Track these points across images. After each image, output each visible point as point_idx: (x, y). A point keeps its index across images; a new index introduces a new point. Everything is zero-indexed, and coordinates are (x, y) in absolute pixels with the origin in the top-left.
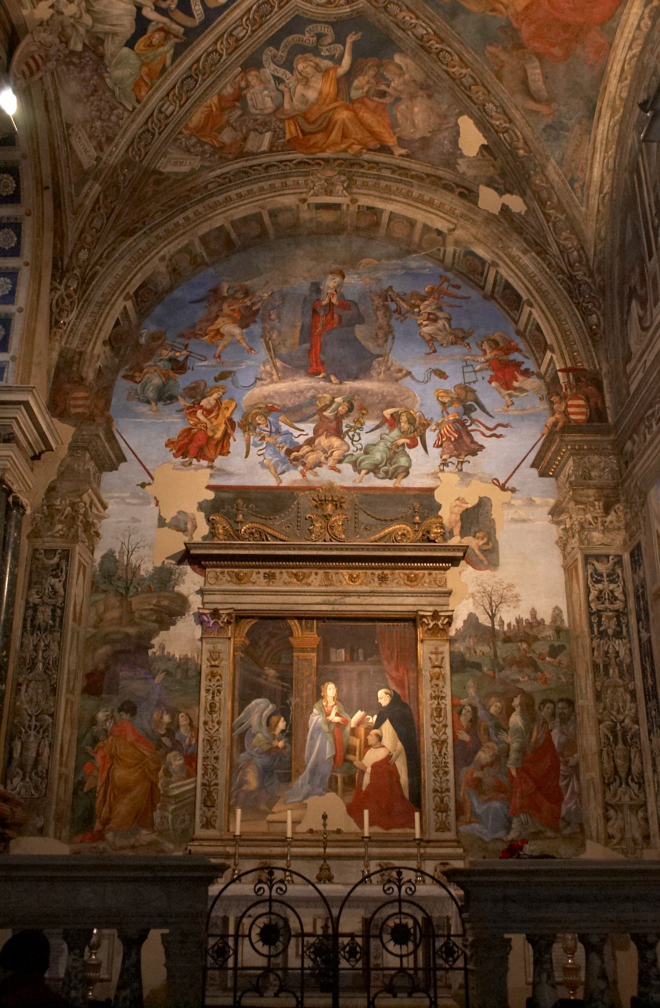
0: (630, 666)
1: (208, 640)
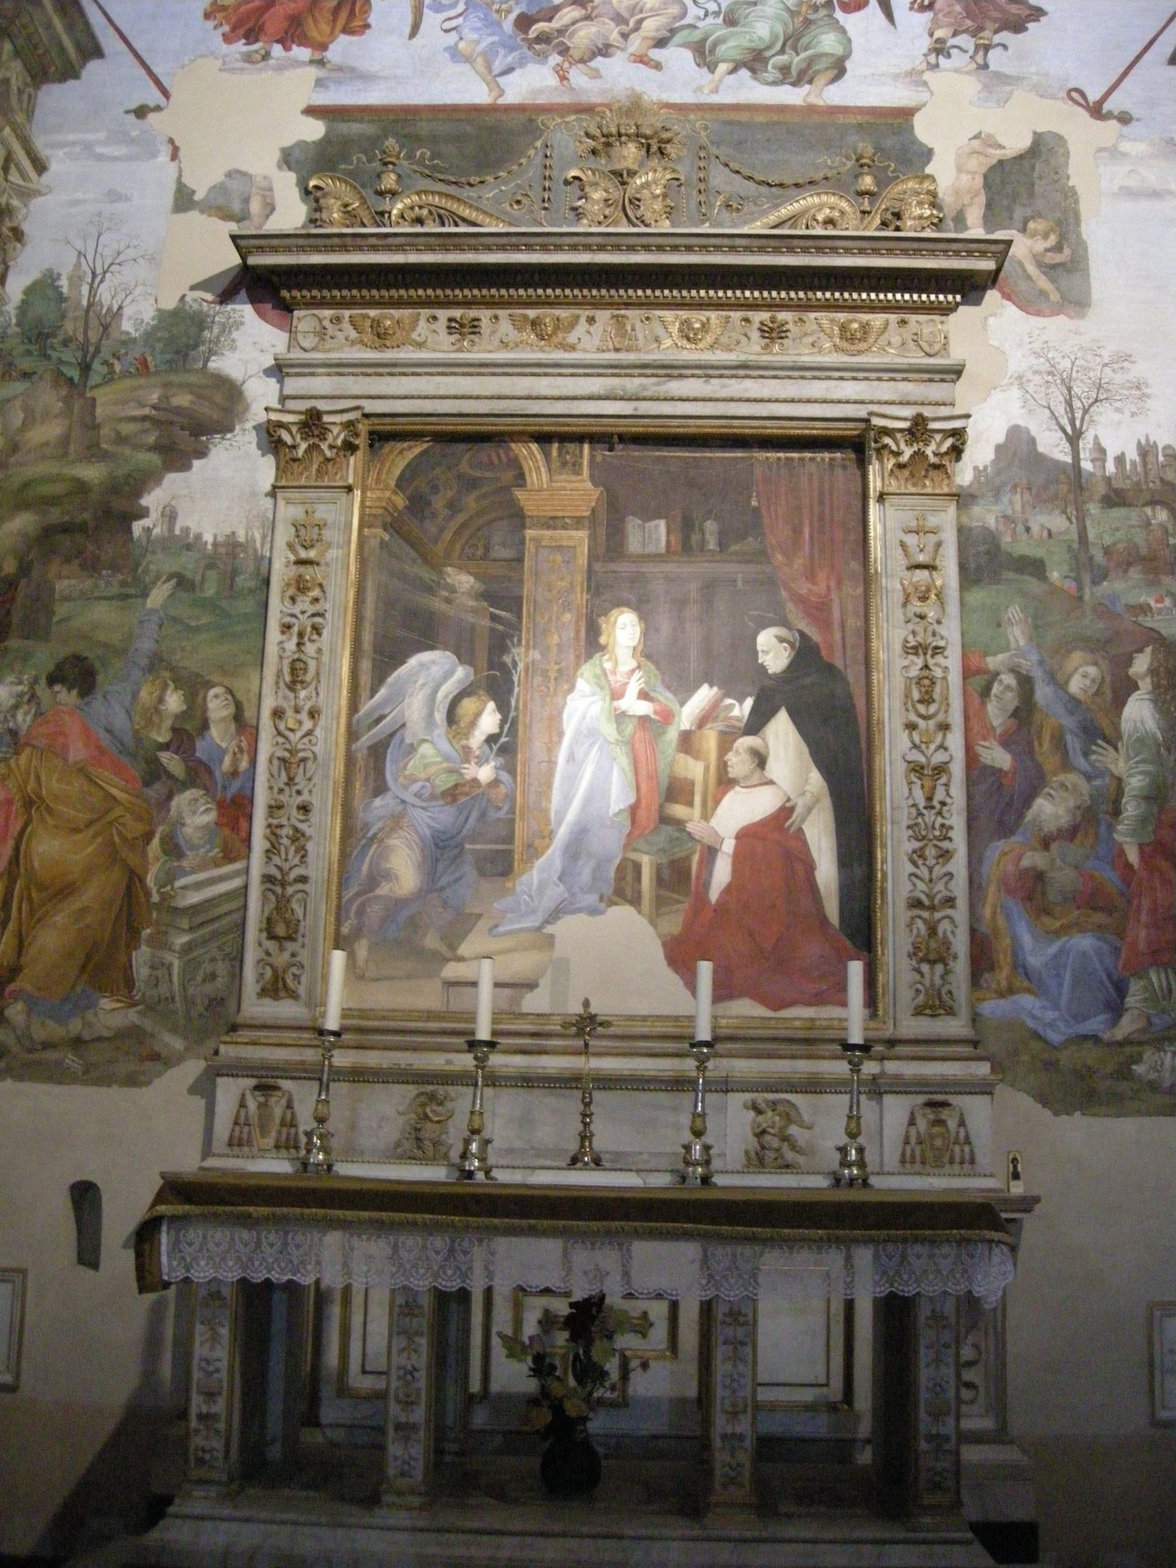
1: (294, 495)
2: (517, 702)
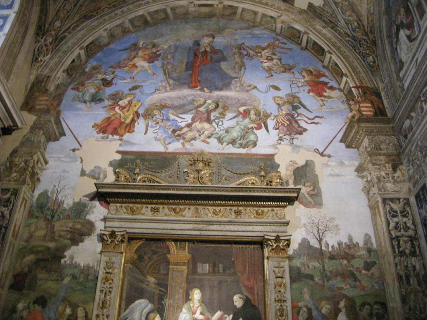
1: (106, 254)
2: (166, 315)
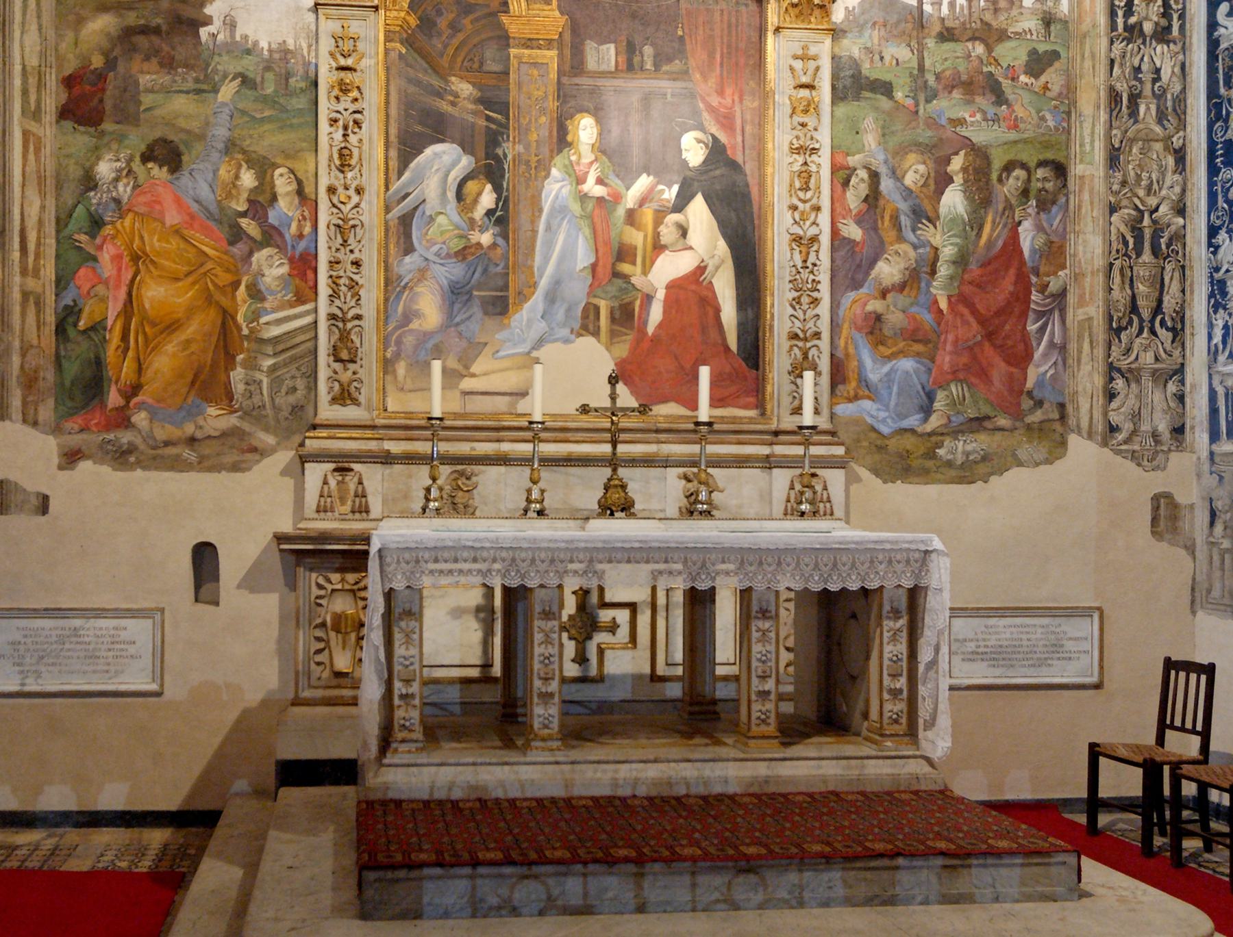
0: (1181, 100)
1: (332, 11)
